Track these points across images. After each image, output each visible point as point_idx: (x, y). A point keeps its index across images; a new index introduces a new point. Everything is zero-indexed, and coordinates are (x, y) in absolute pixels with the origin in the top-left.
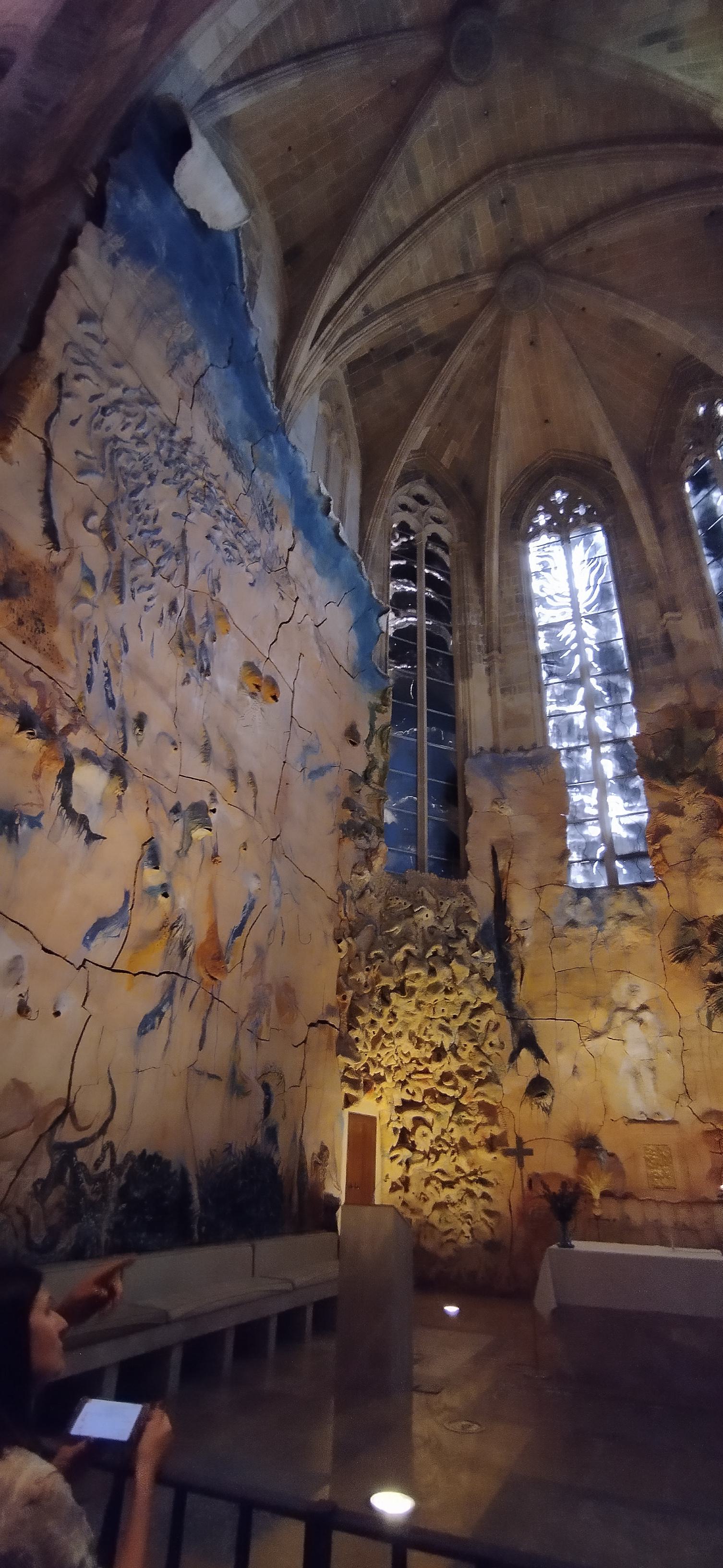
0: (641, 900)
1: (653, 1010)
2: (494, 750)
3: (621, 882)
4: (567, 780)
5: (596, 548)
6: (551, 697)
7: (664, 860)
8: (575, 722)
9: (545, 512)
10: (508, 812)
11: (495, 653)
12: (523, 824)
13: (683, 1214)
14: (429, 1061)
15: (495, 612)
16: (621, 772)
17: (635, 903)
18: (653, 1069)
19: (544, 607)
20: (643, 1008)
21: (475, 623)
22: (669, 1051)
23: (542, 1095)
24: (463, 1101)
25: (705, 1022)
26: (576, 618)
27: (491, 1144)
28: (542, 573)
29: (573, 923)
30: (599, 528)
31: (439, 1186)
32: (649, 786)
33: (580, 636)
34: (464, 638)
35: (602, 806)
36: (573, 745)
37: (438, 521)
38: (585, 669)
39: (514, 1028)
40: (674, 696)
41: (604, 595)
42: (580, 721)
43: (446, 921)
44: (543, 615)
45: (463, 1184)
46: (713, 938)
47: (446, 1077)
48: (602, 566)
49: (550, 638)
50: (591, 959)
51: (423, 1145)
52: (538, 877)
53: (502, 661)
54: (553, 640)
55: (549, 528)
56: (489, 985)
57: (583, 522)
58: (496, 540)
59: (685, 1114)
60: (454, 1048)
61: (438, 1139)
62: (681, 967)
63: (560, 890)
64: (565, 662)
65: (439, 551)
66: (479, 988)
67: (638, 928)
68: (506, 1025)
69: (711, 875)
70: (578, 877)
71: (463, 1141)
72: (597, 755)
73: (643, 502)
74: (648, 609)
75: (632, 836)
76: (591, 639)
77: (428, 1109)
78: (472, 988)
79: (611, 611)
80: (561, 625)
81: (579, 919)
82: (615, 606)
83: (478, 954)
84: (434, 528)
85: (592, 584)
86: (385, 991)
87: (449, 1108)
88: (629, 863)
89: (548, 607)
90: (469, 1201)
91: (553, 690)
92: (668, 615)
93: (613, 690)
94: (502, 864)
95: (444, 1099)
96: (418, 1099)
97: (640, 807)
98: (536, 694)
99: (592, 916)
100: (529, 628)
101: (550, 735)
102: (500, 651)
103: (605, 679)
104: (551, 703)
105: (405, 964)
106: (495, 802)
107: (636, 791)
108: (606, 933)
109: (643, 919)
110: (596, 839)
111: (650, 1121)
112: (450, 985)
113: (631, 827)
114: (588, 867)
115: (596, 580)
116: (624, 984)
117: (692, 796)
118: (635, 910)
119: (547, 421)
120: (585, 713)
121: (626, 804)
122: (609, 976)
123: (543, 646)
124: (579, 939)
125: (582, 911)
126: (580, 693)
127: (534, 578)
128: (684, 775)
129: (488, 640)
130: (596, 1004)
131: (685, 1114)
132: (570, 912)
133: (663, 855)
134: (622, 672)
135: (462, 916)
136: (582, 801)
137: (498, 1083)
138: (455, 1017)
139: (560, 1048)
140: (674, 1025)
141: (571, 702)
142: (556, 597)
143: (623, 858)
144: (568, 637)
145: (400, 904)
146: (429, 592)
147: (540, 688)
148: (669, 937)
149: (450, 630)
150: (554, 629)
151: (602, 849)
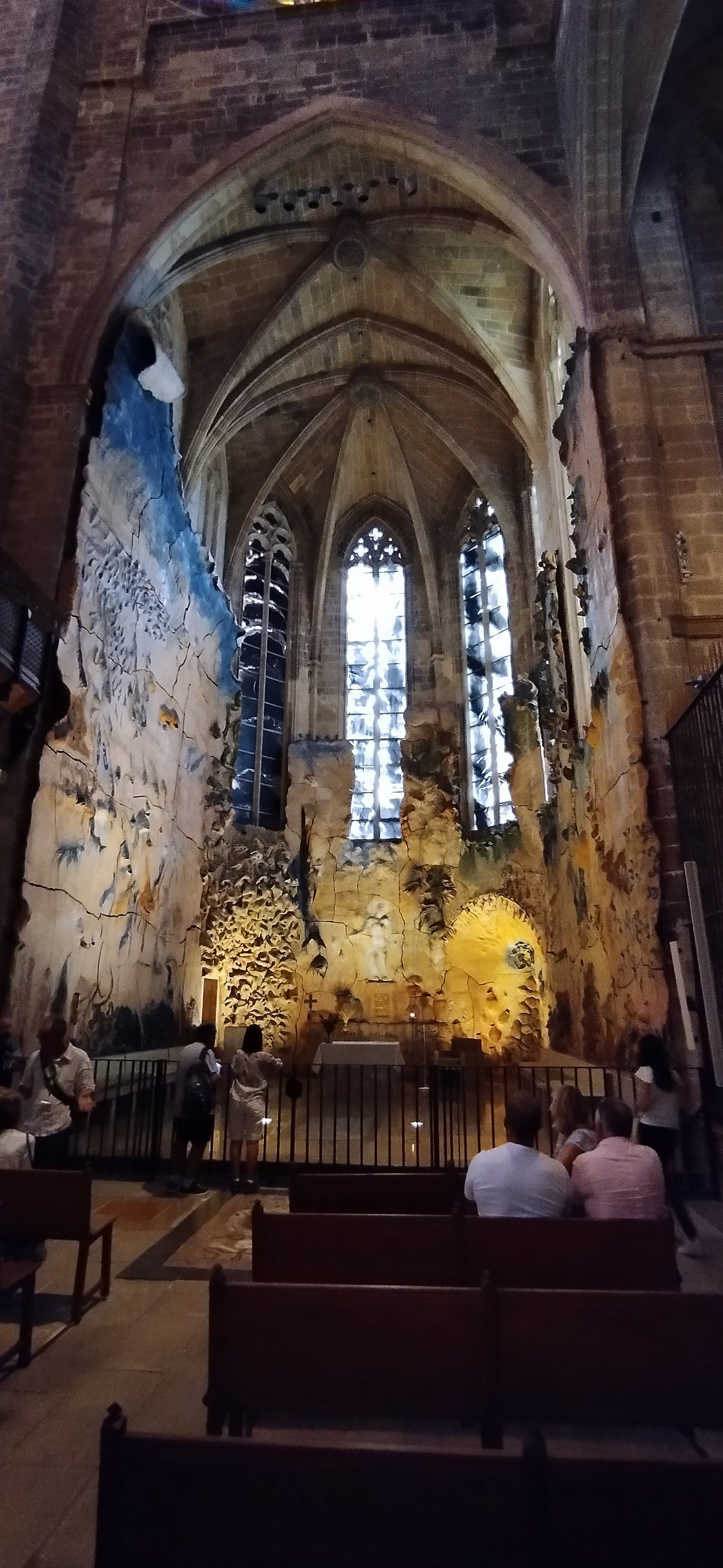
0: (392, 851)
2: (309, 737)
4: (356, 763)
7: (409, 827)
10: (315, 784)
11: (316, 661)
12: (324, 794)
13: (391, 1029)
14: (252, 945)
15: (319, 627)
16: (391, 762)
17: (388, 853)
18: (385, 953)
20: (385, 917)
21: (303, 634)
23: (321, 967)
24: (272, 970)
26: (376, 641)
27: (288, 995)
29: (349, 863)
31: (254, 1019)
32: (407, 779)
34: (295, 646)
35: (376, 785)
37: (282, 540)
38: (377, 683)
39: (306, 927)
40: (429, 718)
42: (369, 723)
43: (269, 860)
45: (269, 1018)
46: (429, 878)
47: (262, 955)
51: (245, 995)
52: (330, 830)
53: (321, 667)
56: (294, 900)
57: (390, 561)
58: (326, 564)
59: (399, 978)
60: (268, 938)
61: (255, 992)
62: (409, 894)
63: (343, 841)
64: (365, 674)
65: (282, 567)
66: (287, 902)
68: (302, 924)
70: (356, 831)
71: (270, 992)
72: (377, 748)
73: (431, 565)
74: (424, 646)
75: (392, 807)
77: (250, 975)
78: (283, 902)
81: (353, 860)
83: (288, 881)
84: (281, 546)
86: (230, 905)
87: (263, 974)
88: (388, 825)
90: (272, 1026)
92: (435, 656)
93: (393, 701)
94: (308, 820)
95: (260, 968)
96: (243, 968)
98: (342, 697)
102: (320, 660)
103: (389, 691)
105: (243, 888)
106: (306, 777)
107: (399, 776)
108: (368, 870)
111: (380, 981)
112: (270, 901)
113: (392, 801)
116: (375, 902)
118: (388, 858)
119: (374, 473)
122: (367, 897)
128: (428, 774)
129: (312, 648)
130: (358, 913)
131: (399, 978)
132: (348, 855)
134: (400, 688)
135: (279, 856)
137: (294, 959)
138: (271, 920)
139: (334, 939)
143: (384, 820)
145: (242, 849)
146: (272, 604)
148: (405, 874)
149: (285, 636)
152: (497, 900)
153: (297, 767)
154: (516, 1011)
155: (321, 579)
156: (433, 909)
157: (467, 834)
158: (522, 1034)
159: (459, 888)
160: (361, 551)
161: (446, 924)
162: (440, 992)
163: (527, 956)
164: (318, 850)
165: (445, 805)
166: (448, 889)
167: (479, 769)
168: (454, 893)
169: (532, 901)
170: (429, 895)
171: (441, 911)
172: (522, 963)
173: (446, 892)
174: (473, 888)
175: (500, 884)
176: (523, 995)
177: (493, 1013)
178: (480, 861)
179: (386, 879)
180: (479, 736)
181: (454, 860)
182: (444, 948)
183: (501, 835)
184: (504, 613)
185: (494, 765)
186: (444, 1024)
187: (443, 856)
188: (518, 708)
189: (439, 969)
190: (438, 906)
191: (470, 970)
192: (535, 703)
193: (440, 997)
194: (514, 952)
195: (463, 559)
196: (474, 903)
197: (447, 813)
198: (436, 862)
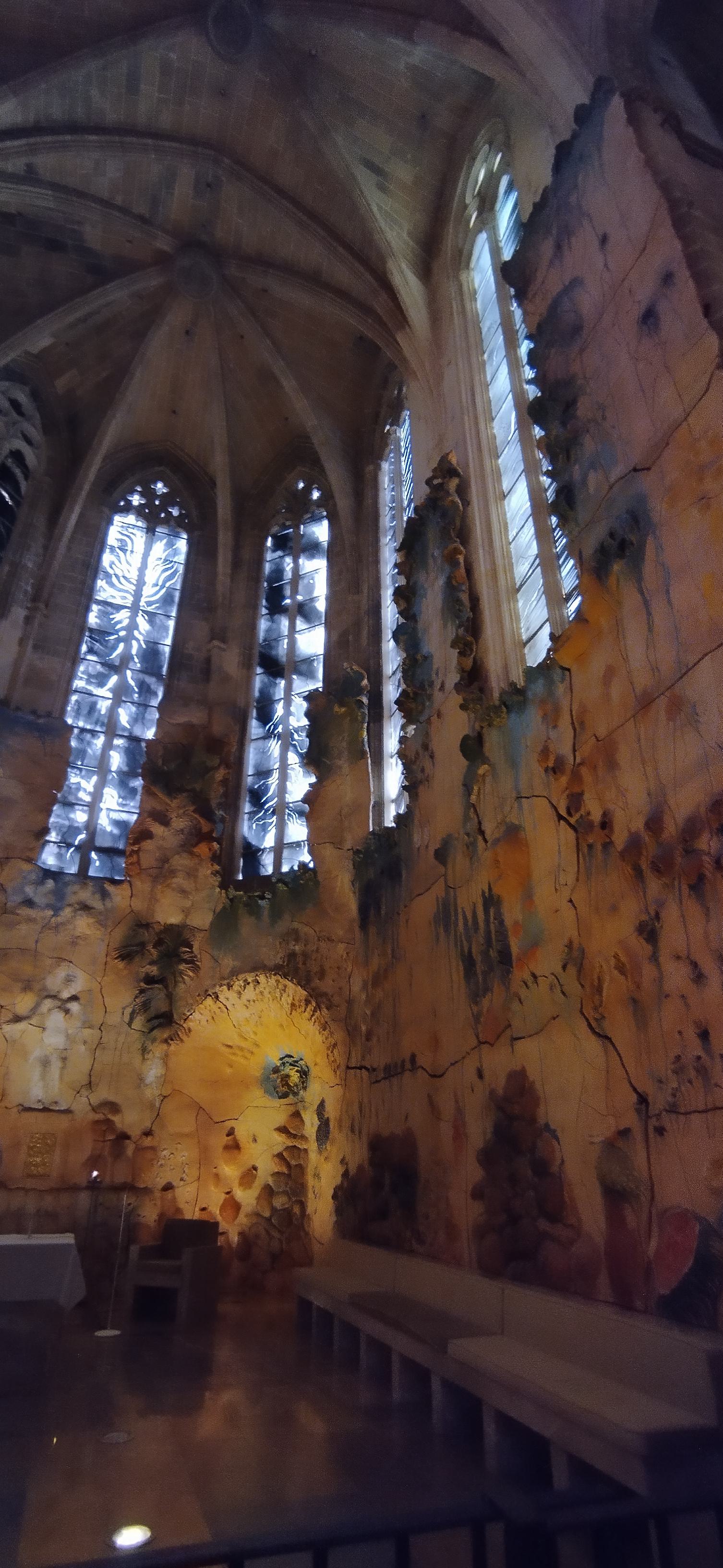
1: (82, 1001)
3: (92, 873)
4: (71, 759)
5: (176, 553)
6: (83, 673)
7: (138, 862)
8: (98, 706)
9: (142, 494)
11: (42, 606)
13: (49, 1202)
15: (56, 564)
16: (125, 769)
17: (98, 896)
18: (64, 1059)
19: (107, 583)
20: (74, 998)
21: (30, 565)
22: (85, 1042)
25: (127, 1018)
26: (135, 608)
28: (117, 550)
29: (29, 903)
30: (185, 536)
32: (147, 790)
33: (133, 626)
35: (97, 796)
36: (88, 727)
38: (126, 659)
40: (195, 716)
41: (167, 600)
42: (103, 706)
44: (104, 591)
46: (158, 943)
48: (176, 571)
49: (103, 615)
50: (37, 942)
53: (46, 616)
54: (105, 619)
55: (139, 512)
58: (84, 493)
62: (121, 965)
63: (26, 867)
64: (110, 645)
67: (91, 920)
69: (174, 885)
70: (49, 858)
72: (108, 746)
73: (230, 534)
74: (201, 629)
75: (116, 831)
76: (140, 633)
79: (169, 617)
80: (119, 608)
81: (37, 900)
82: (174, 614)
85: (160, 583)
88: (103, 856)
89: (112, 585)
91: (87, 667)
92: (216, 643)
93: (145, 690)
97: (134, 807)
98: (69, 665)
99: (52, 900)
100: (86, 596)
101: (69, 709)
102: (47, 606)
103: (141, 676)
104: (81, 679)
107: (133, 791)
108: (59, 919)
109: (100, 913)
110: (80, 825)
111: (45, 1110)
113: (117, 823)
114: (63, 850)
115: (165, 582)
116: (62, 973)
117: (181, 811)
118: (97, 903)
119: (174, 412)
120: (110, 701)
121: (121, 800)
122: (49, 962)
123: (93, 619)
124: (30, 920)
125: (41, 894)
126: (114, 680)
127: (108, 550)
128: (180, 790)
130: (27, 987)
131: (81, 1105)
132: (29, 890)
133: (138, 856)
134: (158, 676)
136: (79, 783)
140: (98, 1018)
141: (101, 684)
142: (122, 579)
143: (101, 850)
144: (120, 622)
147: (76, 660)
148: (119, 935)
150: (109, 609)
151: (82, 836)
152: (267, 982)
154: (267, 1167)
155: (71, 510)
156: (158, 994)
158: (274, 1210)
159: (205, 963)
161: (175, 1016)
162: (148, 1133)
163: (295, 1077)
165: (199, 836)
166: (187, 962)
168: (196, 969)
169: (327, 985)
170: (154, 970)
171: (170, 997)
172: (285, 1089)
173: (182, 967)
174: (228, 962)
175: (276, 957)
176: (280, 1141)
177: (230, 1171)
178: (246, 924)
179: (85, 938)
180: (264, 753)
181: (202, 919)
183: (286, 884)
184: (321, 605)
185: (282, 789)
186: (147, 1191)
187: (186, 912)
188: (336, 708)
189: (151, 1093)
190: (166, 987)
192: (365, 700)
193: (148, 1142)
194: (276, 1070)
195: (269, 542)
196: (230, 987)
197: (203, 849)
198: (174, 919)
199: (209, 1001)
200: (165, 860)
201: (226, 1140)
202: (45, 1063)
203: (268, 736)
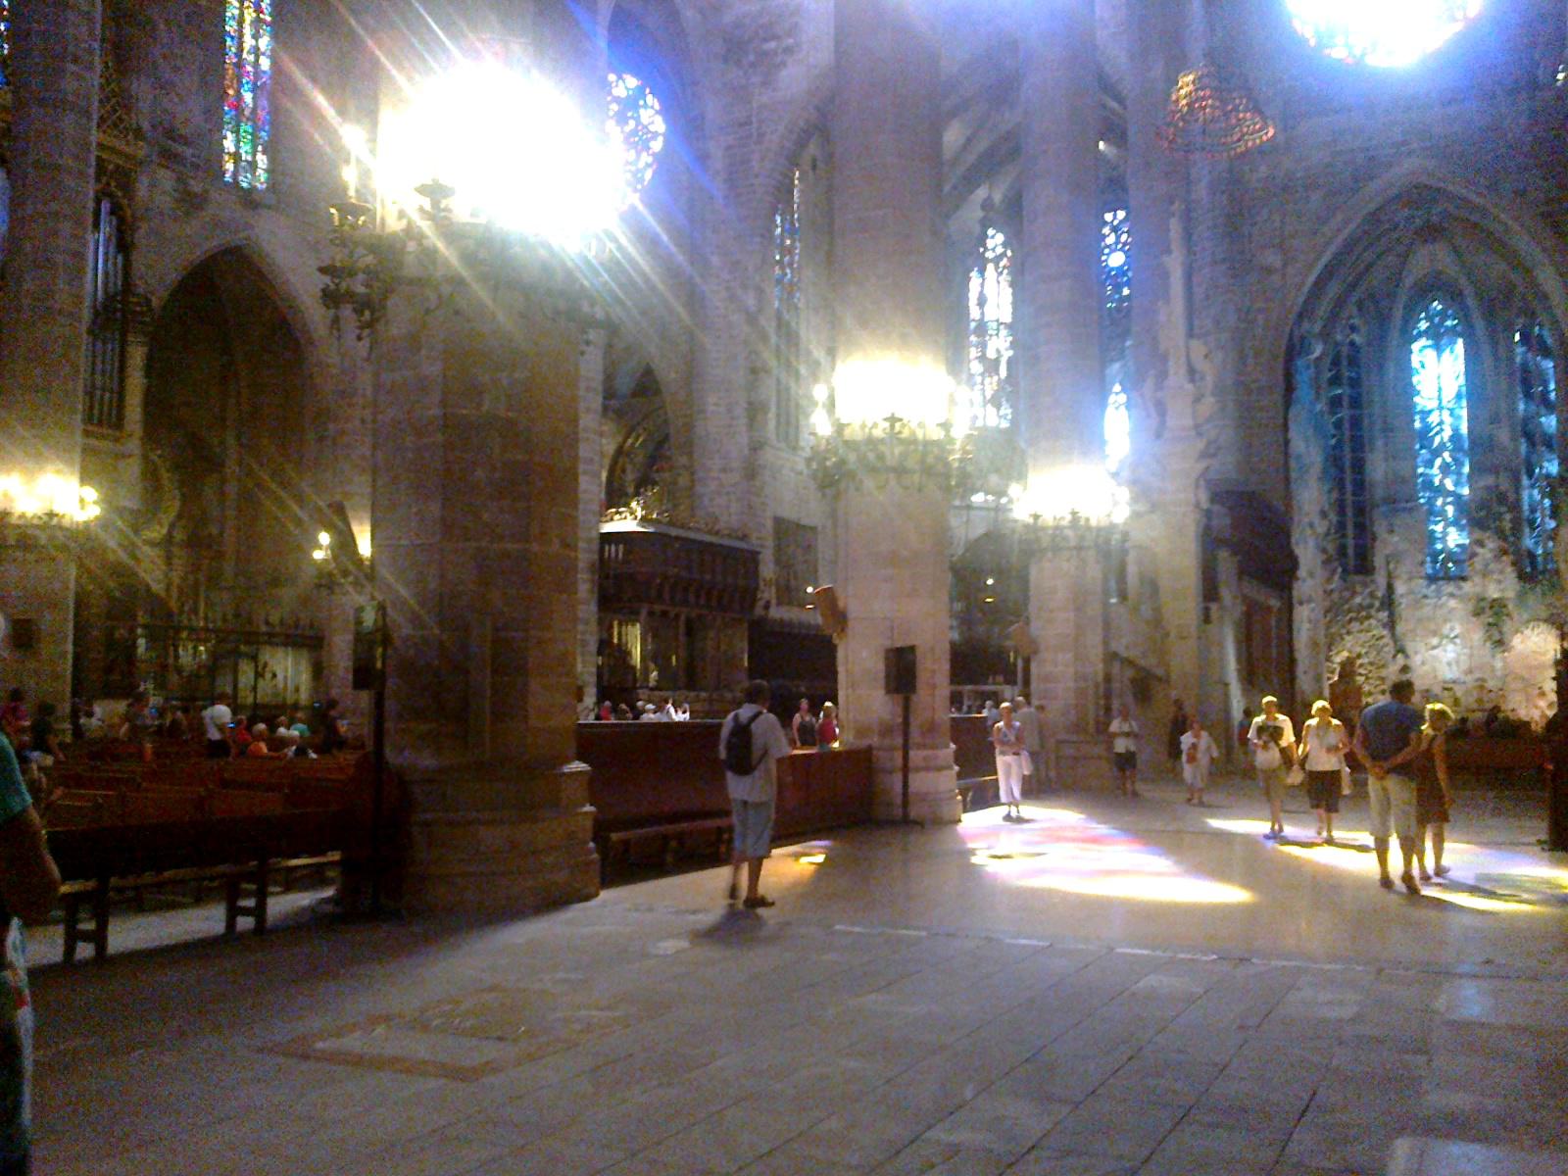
20: (1456, 637)
26: (1440, 408)
35: (1445, 534)
40: (1490, 480)
41: (1459, 396)
46: (1491, 607)
49: (1423, 420)
55: (1426, 333)
62: (1474, 619)
80: (1430, 412)
116: (1448, 626)
123: (1417, 425)
124: (1428, 605)
126: (1438, 462)
130: (1435, 633)
131: (1469, 678)
132: (1425, 591)
135: (1372, 595)
145: (1346, 594)
148: (1470, 606)
152: (1543, 627)
153: (1380, 528)
157: (1522, 576)
159: (1515, 615)
160: (1423, 325)
164: (1400, 588)
165: (1505, 552)
167: (1531, 523)
170: (1491, 620)
171: (1501, 632)
175: (1544, 614)
180: (1531, 496)
181: (1510, 594)
182: (1504, 659)
189: (1499, 673)
191: (1525, 674)
195: (1517, 337)
197: (1505, 558)
198: (1496, 596)
199: (1519, 635)
200: (1487, 565)
201: (1538, 691)
202: (1449, 664)
203: (1532, 486)
